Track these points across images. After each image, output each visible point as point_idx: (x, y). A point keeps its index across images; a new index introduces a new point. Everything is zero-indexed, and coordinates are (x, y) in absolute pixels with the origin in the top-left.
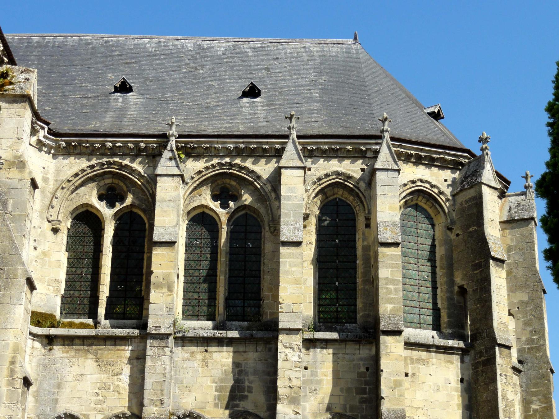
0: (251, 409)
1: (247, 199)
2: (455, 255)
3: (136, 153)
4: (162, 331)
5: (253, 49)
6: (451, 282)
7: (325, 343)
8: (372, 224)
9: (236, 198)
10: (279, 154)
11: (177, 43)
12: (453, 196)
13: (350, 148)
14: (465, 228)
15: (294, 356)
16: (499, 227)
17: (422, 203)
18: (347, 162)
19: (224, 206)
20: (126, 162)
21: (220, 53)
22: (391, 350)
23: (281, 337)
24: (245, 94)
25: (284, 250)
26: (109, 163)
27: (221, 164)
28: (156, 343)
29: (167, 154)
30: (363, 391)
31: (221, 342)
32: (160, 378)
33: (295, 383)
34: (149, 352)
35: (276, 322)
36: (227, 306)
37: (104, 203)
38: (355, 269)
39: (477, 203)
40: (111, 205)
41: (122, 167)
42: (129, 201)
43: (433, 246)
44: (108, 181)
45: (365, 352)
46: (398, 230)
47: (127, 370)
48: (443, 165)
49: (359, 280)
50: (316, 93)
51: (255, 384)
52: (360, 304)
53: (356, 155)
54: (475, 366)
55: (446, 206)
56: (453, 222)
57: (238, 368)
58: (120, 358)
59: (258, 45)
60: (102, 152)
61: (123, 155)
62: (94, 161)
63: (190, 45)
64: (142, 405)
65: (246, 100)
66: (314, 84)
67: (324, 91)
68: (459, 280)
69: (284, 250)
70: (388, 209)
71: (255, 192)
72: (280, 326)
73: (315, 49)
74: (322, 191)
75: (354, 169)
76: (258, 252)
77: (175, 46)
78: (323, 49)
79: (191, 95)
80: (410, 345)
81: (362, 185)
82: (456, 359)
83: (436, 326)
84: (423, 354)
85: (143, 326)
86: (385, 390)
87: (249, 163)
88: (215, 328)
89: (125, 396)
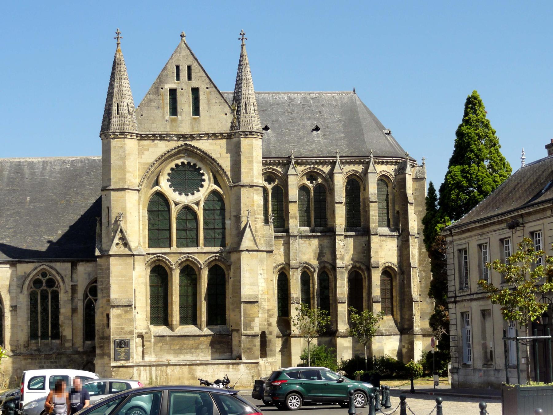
1: (320, 181)
2: (396, 198)
3: (279, 164)
4: (295, 234)
5: (312, 98)
6: (394, 209)
7: (351, 236)
8: (366, 190)
9: (316, 179)
11: (280, 96)
12: (395, 176)
13: (358, 161)
14: (400, 189)
16: (412, 181)
17: (384, 178)
18: (357, 165)
19: (311, 183)
20: (275, 167)
21: (299, 102)
22: (375, 241)
23: (337, 237)
24: (313, 130)
25: (337, 205)
26: (269, 168)
27: (310, 168)
28: (293, 238)
29: (291, 166)
31: (314, 237)
32: (295, 251)
33: (342, 253)
34: (291, 242)
35: (335, 232)
36: (315, 222)
37: (267, 183)
38: (360, 206)
39: (404, 181)
40: (270, 183)
41: (273, 169)
42: (276, 183)
43: (387, 195)
44: (268, 174)
45: (365, 239)
46: (376, 196)
47: (282, 248)
48: (392, 163)
49: (361, 211)
50: (341, 126)
51: (327, 252)
52: (362, 220)
53: (360, 163)
54: (402, 241)
55: (392, 180)
56: (395, 186)
57: (321, 246)
58: (280, 243)
59: (314, 96)
63: (286, 97)
64: (289, 260)
65: (314, 132)
66: (340, 121)
67: (344, 125)
68: (397, 208)
69: (337, 205)
70: (372, 188)
71: (323, 178)
72: (337, 233)
73: (337, 97)
74: (348, 177)
75: (359, 168)
76: (324, 200)
77: (280, 98)
78: (341, 98)
79: (293, 130)
80: (380, 236)
81: (362, 175)
82: (396, 239)
83: (388, 226)
84: (384, 238)
85: (287, 231)
86: (372, 254)
87: (320, 167)
88: (312, 231)
89: (283, 257)
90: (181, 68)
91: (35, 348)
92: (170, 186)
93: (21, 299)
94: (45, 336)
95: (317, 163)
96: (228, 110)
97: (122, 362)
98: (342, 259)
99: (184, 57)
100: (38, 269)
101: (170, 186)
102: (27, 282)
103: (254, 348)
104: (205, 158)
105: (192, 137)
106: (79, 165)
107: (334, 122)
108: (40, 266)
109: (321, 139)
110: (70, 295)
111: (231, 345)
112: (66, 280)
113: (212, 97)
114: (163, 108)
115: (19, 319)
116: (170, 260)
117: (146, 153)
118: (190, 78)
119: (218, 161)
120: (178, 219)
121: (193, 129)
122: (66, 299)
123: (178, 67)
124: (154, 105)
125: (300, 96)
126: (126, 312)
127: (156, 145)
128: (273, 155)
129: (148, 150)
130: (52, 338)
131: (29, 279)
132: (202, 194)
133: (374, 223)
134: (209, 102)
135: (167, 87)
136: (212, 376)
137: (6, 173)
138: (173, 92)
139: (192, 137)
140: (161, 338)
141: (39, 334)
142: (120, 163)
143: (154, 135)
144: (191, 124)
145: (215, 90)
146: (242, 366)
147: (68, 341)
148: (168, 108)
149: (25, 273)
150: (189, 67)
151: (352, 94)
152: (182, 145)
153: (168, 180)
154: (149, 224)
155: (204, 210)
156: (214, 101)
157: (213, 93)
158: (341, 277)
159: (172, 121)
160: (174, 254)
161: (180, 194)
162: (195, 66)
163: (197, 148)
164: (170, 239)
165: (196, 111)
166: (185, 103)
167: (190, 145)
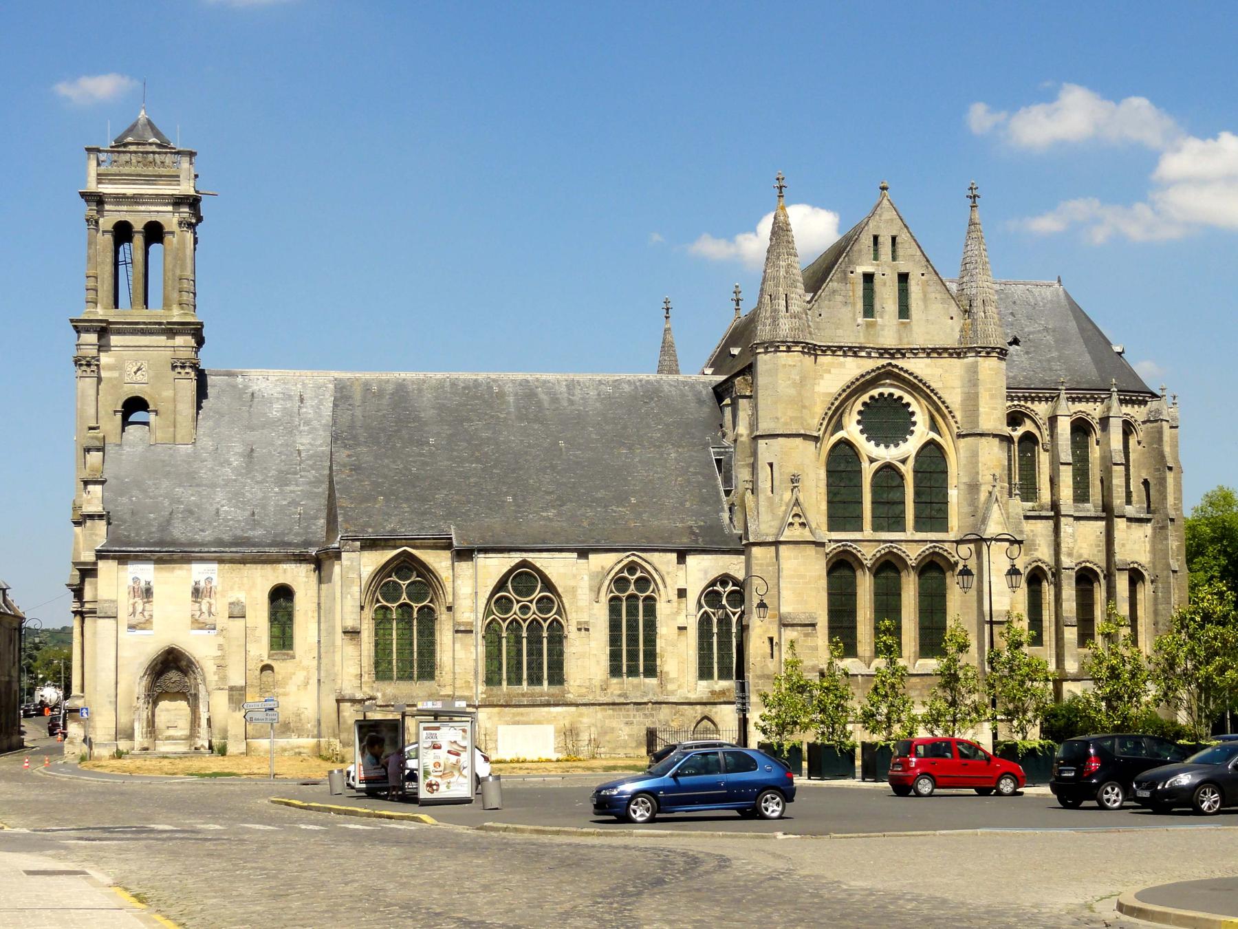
15: (1070, 530)
33: (1071, 545)
50: (1050, 338)
87: (1029, 404)
90: (881, 239)
92: (862, 432)
93: (595, 611)
94: (633, 672)
96: (954, 310)
98: (1070, 555)
99: (887, 221)
101: (862, 432)
102: (607, 583)
105: (901, 353)
106: (627, 388)
109: (1024, 358)
114: (854, 304)
115: (593, 644)
116: (863, 551)
117: (826, 376)
118: (894, 259)
119: (941, 394)
120: (875, 486)
123: (876, 238)
124: (839, 298)
126: (807, 635)
127: (842, 365)
129: (829, 372)
130: (646, 676)
132: (911, 446)
134: (925, 299)
135: (861, 269)
137: (511, 399)
138: (868, 278)
139: (901, 353)
141: (641, 669)
142: (792, 392)
144: (899, 331)
145: (935, 278)
147: (672, 681)
148: (860, 306)
150: (894, 239)
151: (1057, 285)
152: (883, 366)
153: (859, 422)
154: (829, 492)
155: (916, 472)
156: (933, 296)
158: (1069, 584)
159: (869, 325)
160: (868, 542)
162: (903, 237)
163: (906, 371)
164: (860, 517)
165: (904, 311)
167: (896, 366)
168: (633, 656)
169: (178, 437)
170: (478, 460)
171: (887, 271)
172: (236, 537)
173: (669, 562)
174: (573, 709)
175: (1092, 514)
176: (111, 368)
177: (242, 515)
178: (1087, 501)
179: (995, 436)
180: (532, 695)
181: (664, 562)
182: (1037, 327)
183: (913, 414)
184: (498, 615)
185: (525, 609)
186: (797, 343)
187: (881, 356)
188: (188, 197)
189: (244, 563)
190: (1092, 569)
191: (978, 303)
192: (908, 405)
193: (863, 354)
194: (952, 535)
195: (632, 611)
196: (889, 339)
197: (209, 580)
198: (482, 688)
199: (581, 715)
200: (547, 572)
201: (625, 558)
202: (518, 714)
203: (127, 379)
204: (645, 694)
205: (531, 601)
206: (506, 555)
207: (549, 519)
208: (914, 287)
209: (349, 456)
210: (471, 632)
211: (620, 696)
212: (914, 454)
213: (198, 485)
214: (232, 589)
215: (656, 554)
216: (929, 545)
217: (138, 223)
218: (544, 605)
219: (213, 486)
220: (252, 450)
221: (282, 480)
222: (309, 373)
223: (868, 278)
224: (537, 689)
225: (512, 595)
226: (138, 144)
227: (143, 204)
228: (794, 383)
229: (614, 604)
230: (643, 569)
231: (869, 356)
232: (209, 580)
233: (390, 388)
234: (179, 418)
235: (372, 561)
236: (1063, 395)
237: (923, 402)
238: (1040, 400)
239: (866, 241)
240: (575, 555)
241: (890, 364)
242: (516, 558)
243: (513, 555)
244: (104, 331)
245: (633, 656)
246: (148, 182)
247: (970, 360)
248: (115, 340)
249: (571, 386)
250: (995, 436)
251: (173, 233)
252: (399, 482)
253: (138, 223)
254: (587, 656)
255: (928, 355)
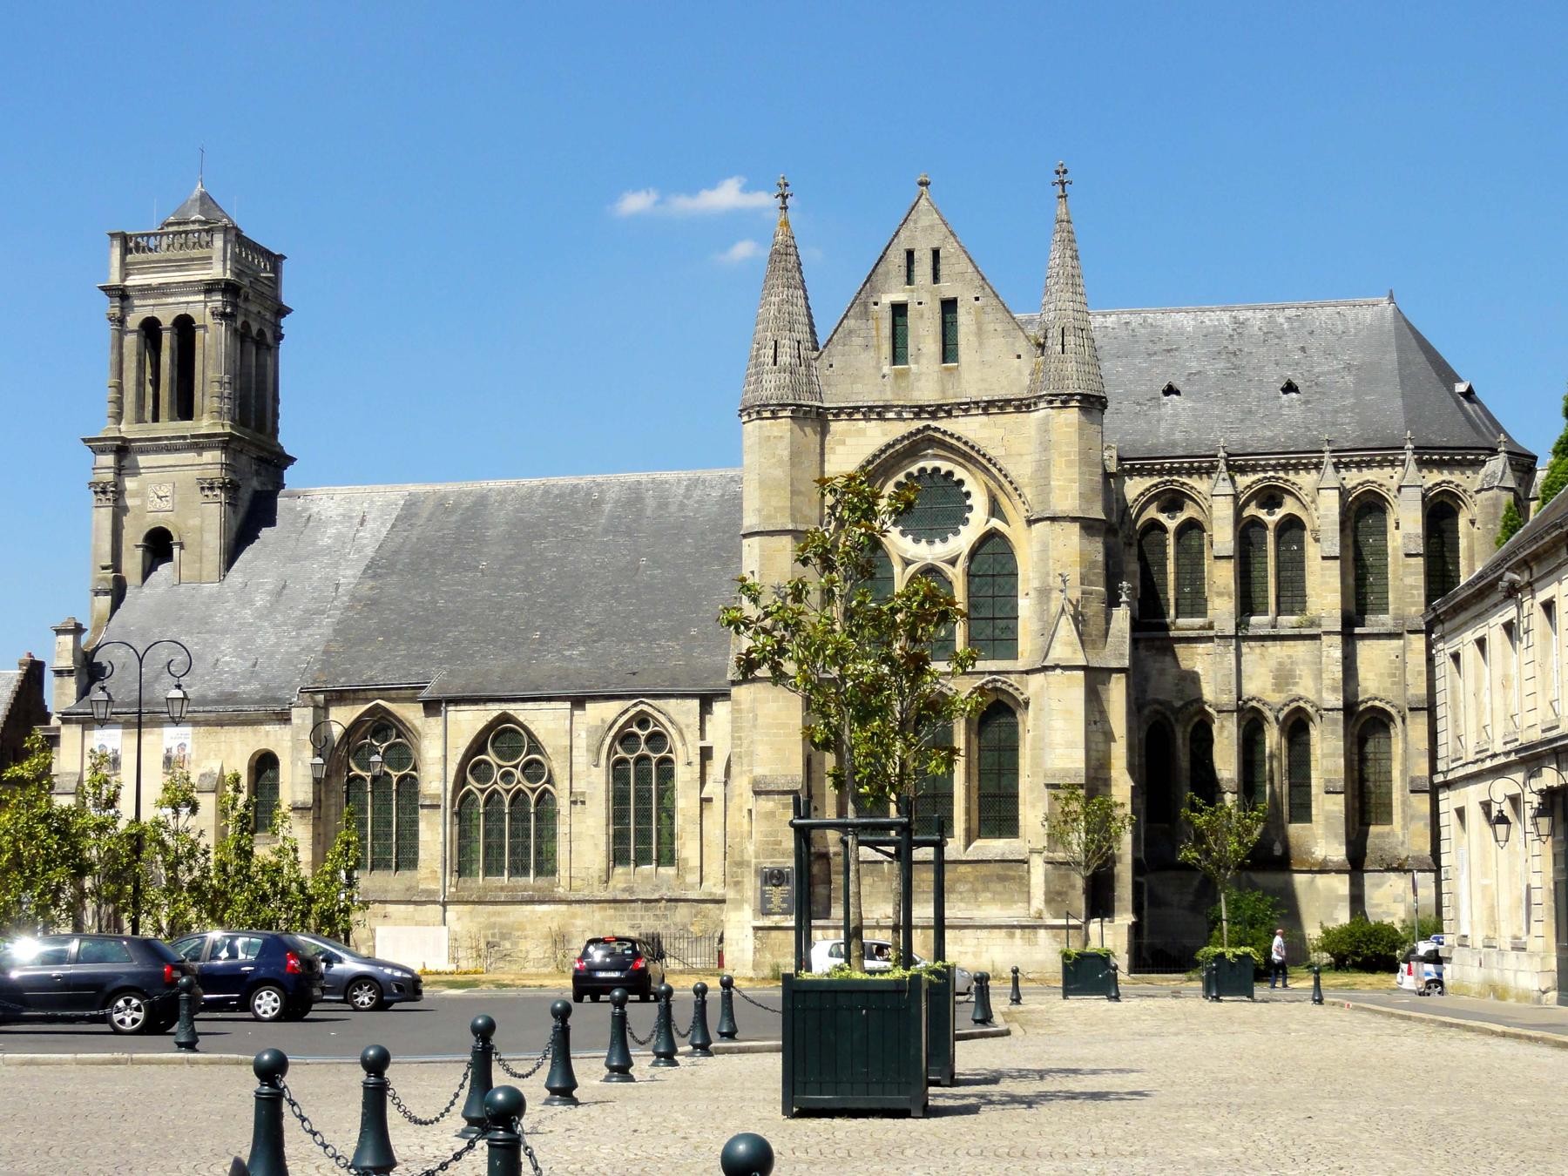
0: (1302, 693)
5: (1289, 319)
10: (1317, 466)
30: (1394, 675)
46: (1420, 541)
50: (1349, 379)
60: (1160, 473)
61: (1179, 473)
62: (1156, 480)
87: (1292, 476)
90: (916, 255)
91: (621, 885)
94: (643, 858)
95: (1285, 468)
96: (1022, 346)
97: (777, 918)
99: (924, 229)
100: (632, 712)
102: (608, 741)
103: (1071, 893)
104: (970, 456)
107: (1337, 371)
108: (635, 705)
110: (697, 768)
111: (1028, 886)
112: (688, 737)
113: (987, 318)
114: (878, 348)
115: (590, 822)
117: (840, 449)
118: (936, 279)
119: (1001, 463)
121: (943, 392)
122: (688, 777)
123: (910, 254)
125: (1259, 315)
127: (861, 432)
128: (1180, 452)
129: (844, 443)
131: (612, 733)
132: (963, 540)
133: (1414, 604)
134: (980, 332)
135: (887, 299)
136: (975, 954)
138: (899, 310)
140: (871, 867)
143: (857, 409)
144: (942, 382)
145: (995, 302)
146: (1042, 932)
149: (603, 721)
150: (936, 253)
152: (919, 431)
155: (970, 575)
156: (991, 327)
157: (988, 309)
159: (900, 376)
161: (917, 541)
163: (952, 436)
165: (949, 351)
166: (924, 332)
167: (936, 429)
168: (643, 836)
169: (205, 573)
170: (528, 587)
171: (925, 298)
172: (222, 693)
173: (688, 712)
174: (563, 908)
175: (1390, 628)
176: (136, 494)
177: (241, 666)
178: (1386, 611)
179: (1074, 519)
180: (514, 889)
181: (684, 711)
182: (1336, 365)
183: (968, 495)
184: (472, 785)
185: (507, 776)
186: (784, 406)
187: (917, 416)
188: (218, 282)
189: (222, 725)
190: (1383, 711)
191: (1055, 333)
192: (961, 483)
193: (891, 415)
194: (1021, 664)
195: (643, 777)
196: (927, 393)
197: (182, 746)
198: (451, 879)
199: (574, 916)
200: (532, 728)
201: (631, 708)
202: (494, 914)
203: (150, 507)
204: (657, 887)
205: (516, 767)
206: (481, 707)
207: (571, 658)
208: (964, 318)
209: (372, 588)
210: (438, 806)
211: (624, 890)
212: (966, 551)
213: (209, 632)
214: (207, 757)
215: (673, 702)
216: (988, 678)
217: (166, 320)
218: (534, 770)
219: (224, 632)
220: (284, 587)
221: (303, 624)
222: (381, 488)
223: (899, 310)
224: (521, 881)
225: (491, 757)
226: (179, 224)
227: (172, 294)
228: (781, 461)
229: (618, 770)
230: (657, 723)
231: (900, 418)
232: (182, 746)
233: (468, 502)
234: (205, 551)
235: (341, 718)
236: (1328, 459)
237: (982, 476)
238: (1306, 468)
239: (897, 259)
240: (568, 705)
241: (928, 427)
242: (494, 710)
243: (490, 706)
244: (123, 450)
245: (643, 836)
246: (180, 268)
247: (1041, 413)
248: (142, 460)
249: (693, 484)
250: (1074, 519)
251: (204, 327)
252: (412, 618)
253: (166, 318)
254: (583, 835)
255: (986, 412)
